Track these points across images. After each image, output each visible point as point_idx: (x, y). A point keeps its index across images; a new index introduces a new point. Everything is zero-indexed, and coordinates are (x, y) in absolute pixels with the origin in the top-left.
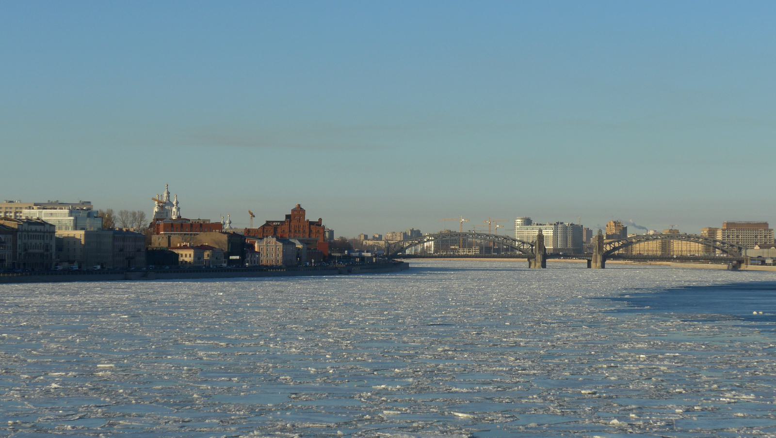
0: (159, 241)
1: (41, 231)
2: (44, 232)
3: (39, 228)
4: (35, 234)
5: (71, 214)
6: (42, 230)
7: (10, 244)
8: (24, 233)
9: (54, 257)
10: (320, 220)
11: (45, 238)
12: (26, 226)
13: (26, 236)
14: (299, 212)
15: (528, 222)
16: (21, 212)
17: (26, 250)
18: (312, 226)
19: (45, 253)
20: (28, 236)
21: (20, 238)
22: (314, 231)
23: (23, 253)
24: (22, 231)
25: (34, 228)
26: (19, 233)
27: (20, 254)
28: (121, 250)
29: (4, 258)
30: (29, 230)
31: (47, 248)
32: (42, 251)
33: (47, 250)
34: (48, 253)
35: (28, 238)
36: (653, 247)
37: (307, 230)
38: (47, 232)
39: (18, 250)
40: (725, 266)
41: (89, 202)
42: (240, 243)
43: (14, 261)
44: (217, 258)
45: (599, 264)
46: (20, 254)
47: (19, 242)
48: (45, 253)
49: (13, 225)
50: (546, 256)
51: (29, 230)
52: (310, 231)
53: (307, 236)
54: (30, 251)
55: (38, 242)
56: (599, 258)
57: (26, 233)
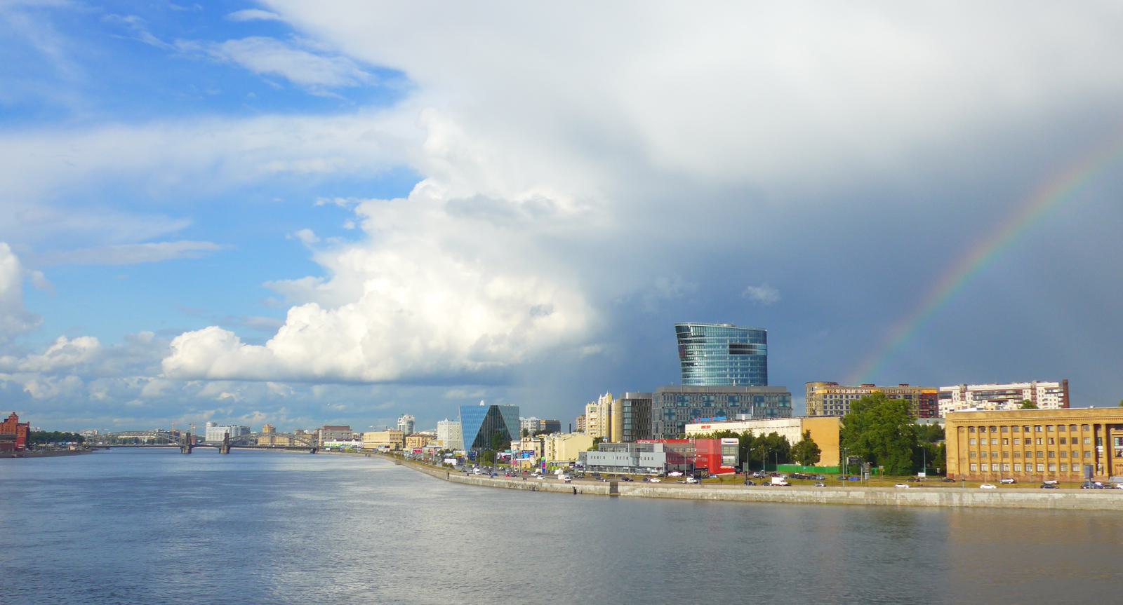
10: (29, 423)
15: (215, 425)
18: (18, 427)
22: (19, 430)
36: (285, 441)
37: (15, 430)
40: (309, 452)
45: (225, 451)
50: (191, 446)
52: (17, 430)
53: (14, 433)
56: (226, 447)
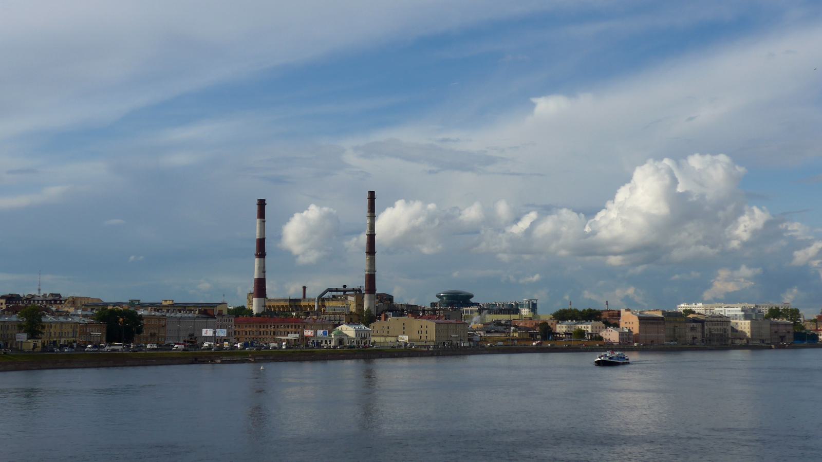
0: (810, 327)
1: (720, 321)
2: (723, 322)
3: (719, 319)
5: (742, 311)
7: (699, 329)
9: (730, 336)
12: (710, 319)
16: (713, 310)
17: (710, 332)
24: (708, 321)
25: (715, 319)
26: (705, 322)
27: (707, 334)
28: (776, 332)
31: (725, 330)
32: (721, 333)
33: (725, 332)
34: (726, 334)
38: (725, 322)
39: (705, 332)
46: (707, 334)
47: (706, 327)
49: (701, 318)
55: (719, 327)
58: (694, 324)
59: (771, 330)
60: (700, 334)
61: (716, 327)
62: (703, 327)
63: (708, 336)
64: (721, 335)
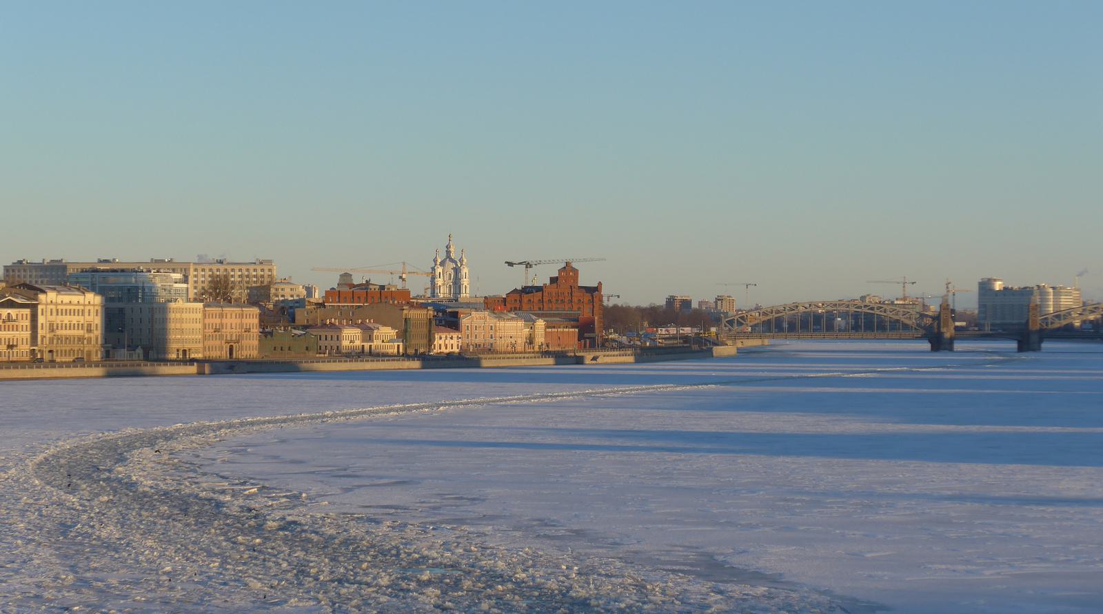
4: (68, 307)
6: (82, 302)
7: (27, 323)
8: (50, 307)
11: (87, 314)
13: (54, 311)
14: (569, 271)
19: (86, 336)
20: (57, 310)
21: (42, 314)
23: (48, 336)
27: (43, 337)
29: (15, 344)
30: (59, 302)
32: (81, 332)
34: (92, 335)
35: (57, 314)
39: (40, 331)
41: (270, 262)
42: (830, 317)
43: (32, 348)
44: (383, 341)
46: (43, 337)
47: (41, 320)
48: (86, 336)
51: (59, 302)
54: (59, 332)
57: (53, 307)
58: (9, 311)
59: (205, 325)
60: (27, 334)
61: (66, 319)
62: (34, 318)
63: (47, 341)
64: (81, 339)
